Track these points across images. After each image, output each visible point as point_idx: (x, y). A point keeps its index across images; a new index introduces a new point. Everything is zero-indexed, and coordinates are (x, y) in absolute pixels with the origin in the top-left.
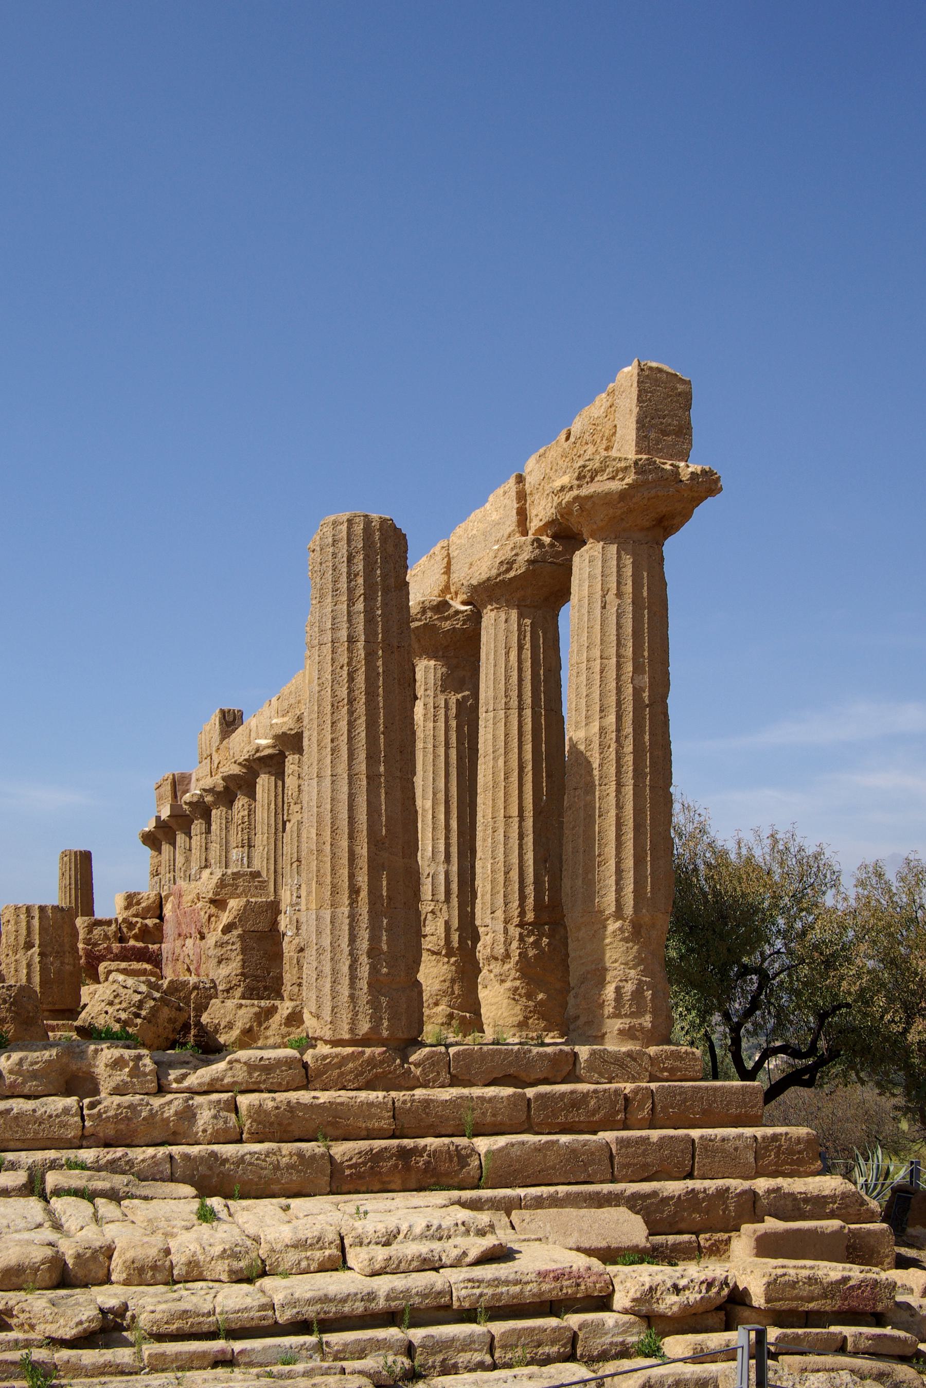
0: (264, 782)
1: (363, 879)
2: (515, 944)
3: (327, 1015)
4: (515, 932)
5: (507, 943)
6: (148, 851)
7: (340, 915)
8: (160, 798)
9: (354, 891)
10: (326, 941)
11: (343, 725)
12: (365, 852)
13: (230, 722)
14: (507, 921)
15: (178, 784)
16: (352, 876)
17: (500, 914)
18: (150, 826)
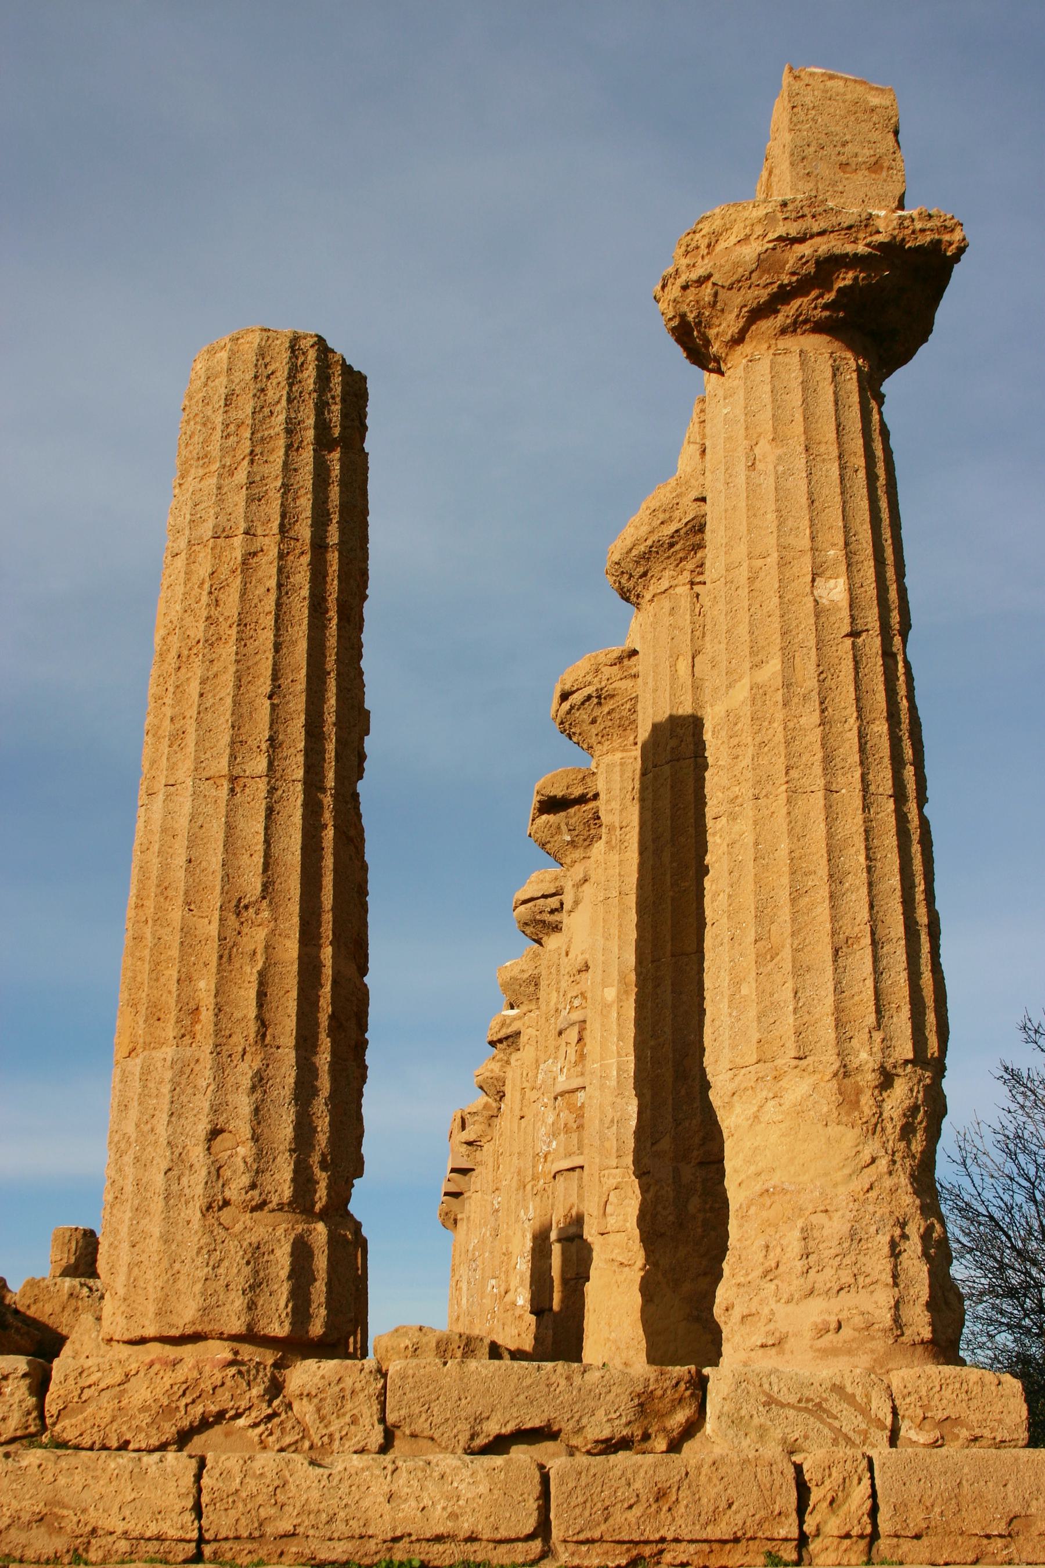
1: (205, 986)
7: (159, 1065)
12: (213, 929)
16: (185, 980)
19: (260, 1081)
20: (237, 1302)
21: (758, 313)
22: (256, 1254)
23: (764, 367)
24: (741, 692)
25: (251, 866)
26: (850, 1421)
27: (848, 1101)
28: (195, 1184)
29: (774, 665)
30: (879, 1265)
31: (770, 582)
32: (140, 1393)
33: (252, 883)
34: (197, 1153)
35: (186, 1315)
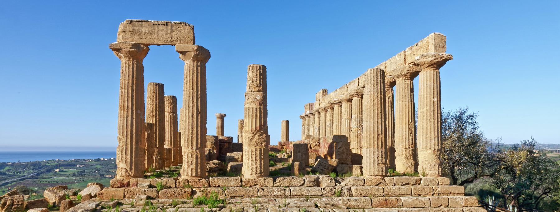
0: (336, 107)
1: (376, 143)
2: (404, 153)
3: (368, 170)
4: (403, 149)
5: (402, 153)
6: (302, 120)
8: (306, 108)
9: (374, 145)
10: (368, 155)
11: (372, 111)
13: (325, 92)
14: (402, 147)
15: (311, 106)
17: (401, 146)
18: (303, 115)
19: (382, 152)
20: (381, 172)
21: (428, 66)
22: (382, 168)
23: (429, 72)
24: (425, 109)
25: (380, 130)
26: (434, 182)
27: (434, 153)
28: (376, 162)
29: (428, 108)
30: (437, 168)
31: (429, 98)
32: (373, 181)
33: (380, 132)
34: (376, 159)
35: (376, 174)
